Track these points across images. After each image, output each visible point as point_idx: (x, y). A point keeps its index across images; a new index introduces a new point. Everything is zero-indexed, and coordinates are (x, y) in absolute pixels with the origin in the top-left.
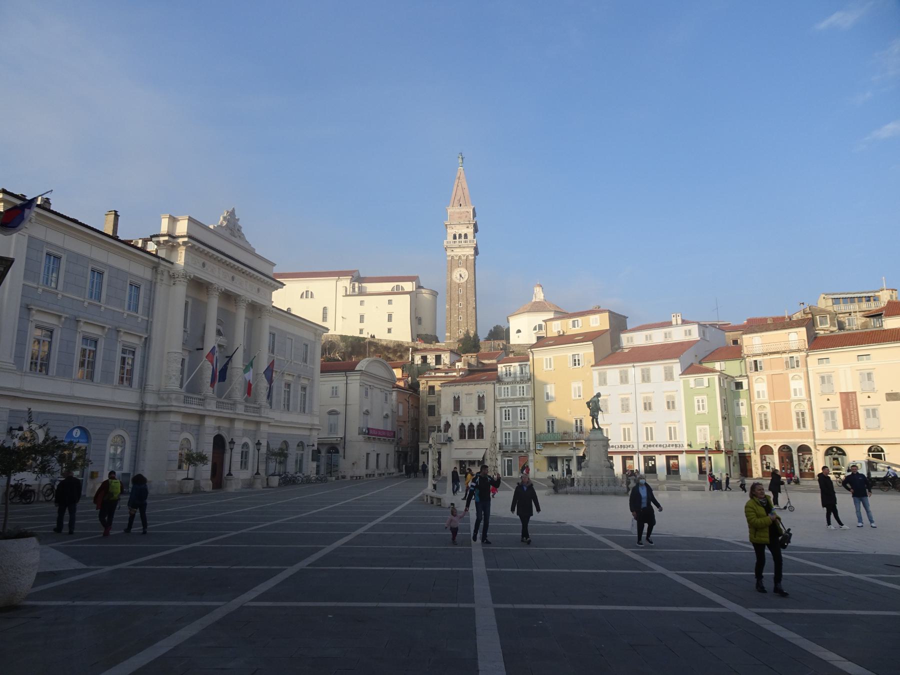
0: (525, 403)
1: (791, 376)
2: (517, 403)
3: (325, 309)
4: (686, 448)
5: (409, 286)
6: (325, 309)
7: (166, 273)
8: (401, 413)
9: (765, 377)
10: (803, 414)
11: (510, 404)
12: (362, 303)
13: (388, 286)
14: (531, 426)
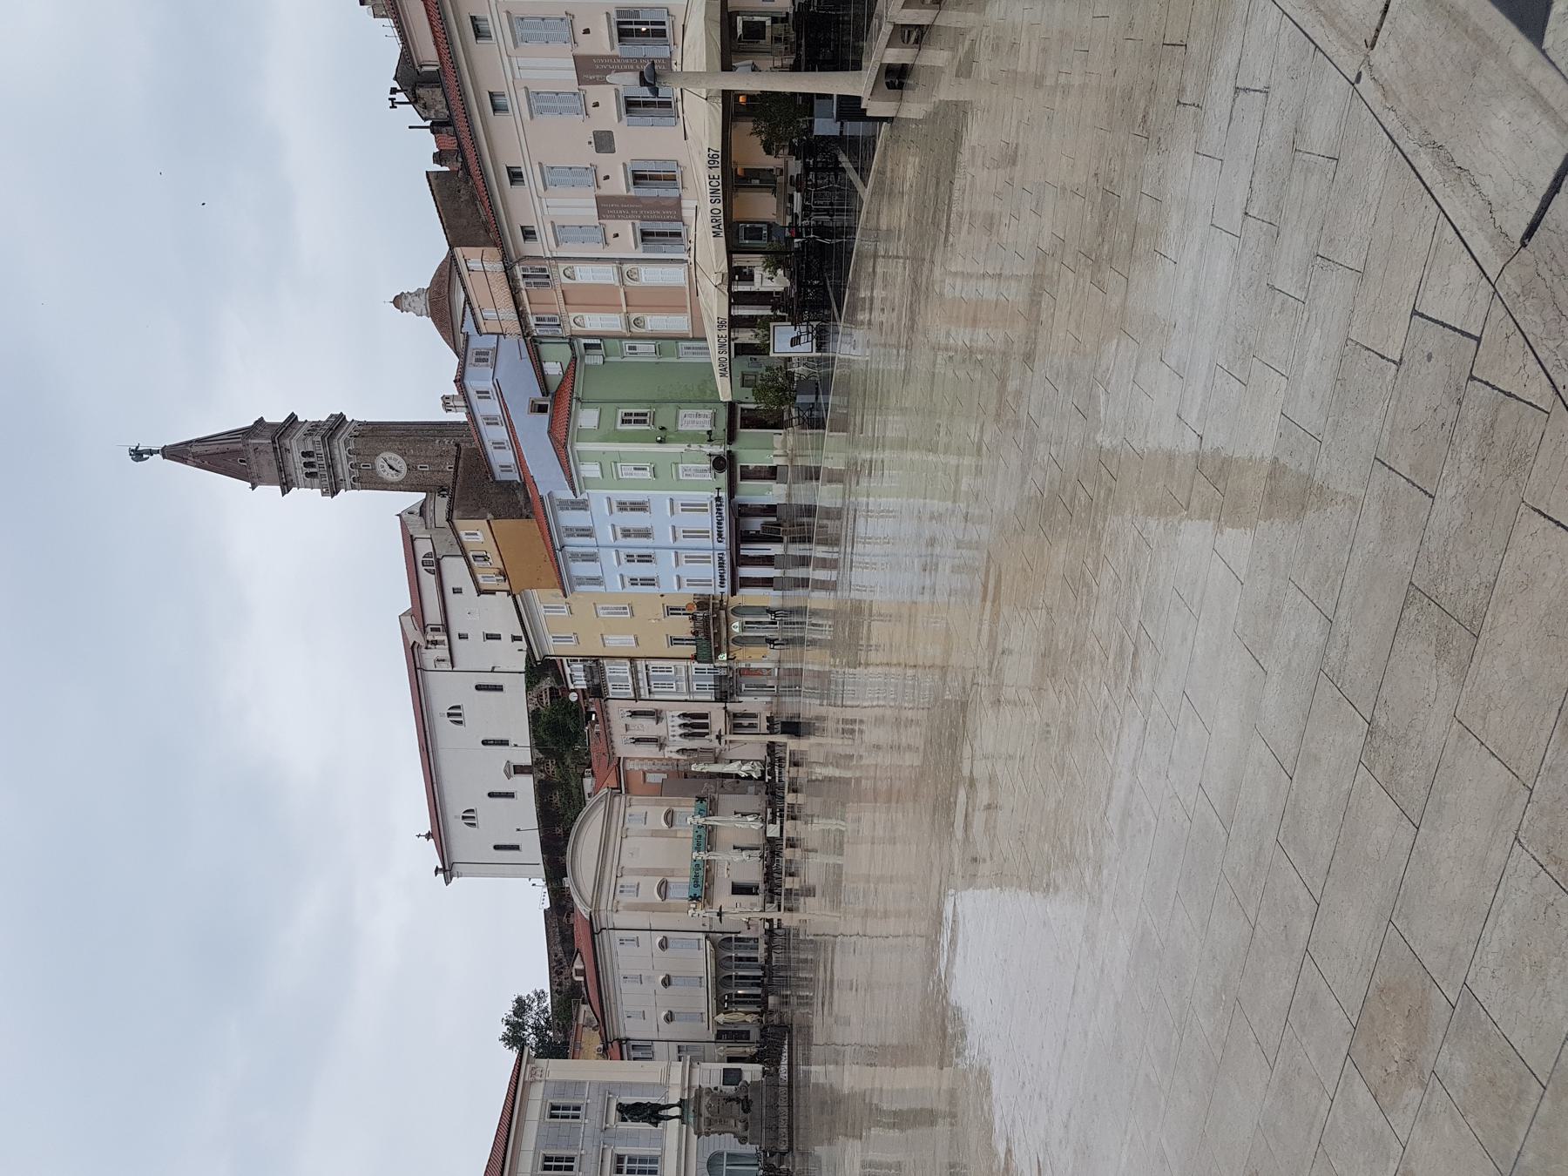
3: (478, 688)
4: (723, 494)
5: (423, 547)
6: (478, 688)
9: (572, 315)
11: (643, 684)
12: (462, 637)
13: (428, 581)
14: (684, 663)
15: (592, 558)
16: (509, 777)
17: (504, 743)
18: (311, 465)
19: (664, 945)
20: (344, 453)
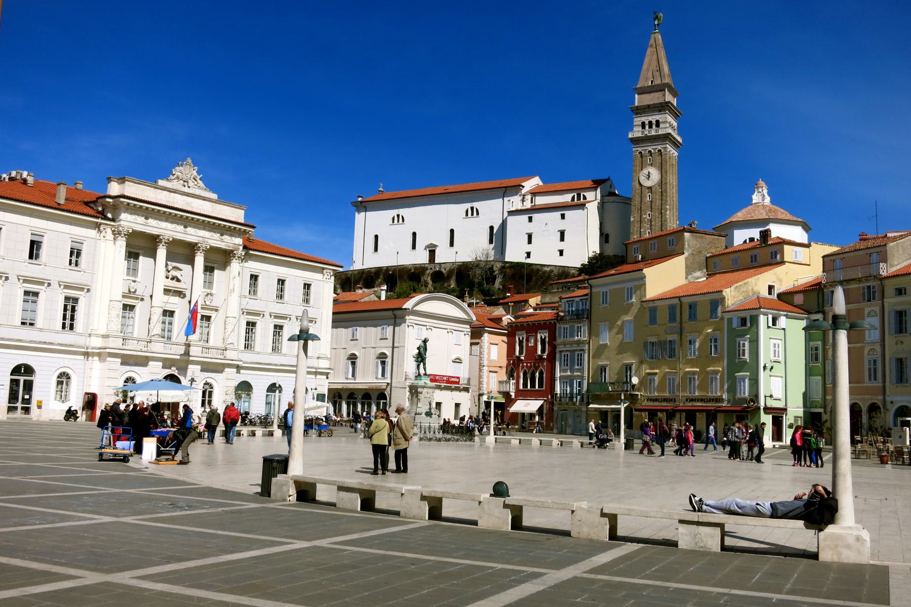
1: (867, 310)
2: (575, 347)
7: (109, 231)
10: (875, 361)
12: (530, 219)
13: (567, 198)
14: (586, 375)
15: (672, 318)
16: (427, 247)
17: (452, 244)
18: (651, 127)
19: (382, 357)
20: (659, 147)
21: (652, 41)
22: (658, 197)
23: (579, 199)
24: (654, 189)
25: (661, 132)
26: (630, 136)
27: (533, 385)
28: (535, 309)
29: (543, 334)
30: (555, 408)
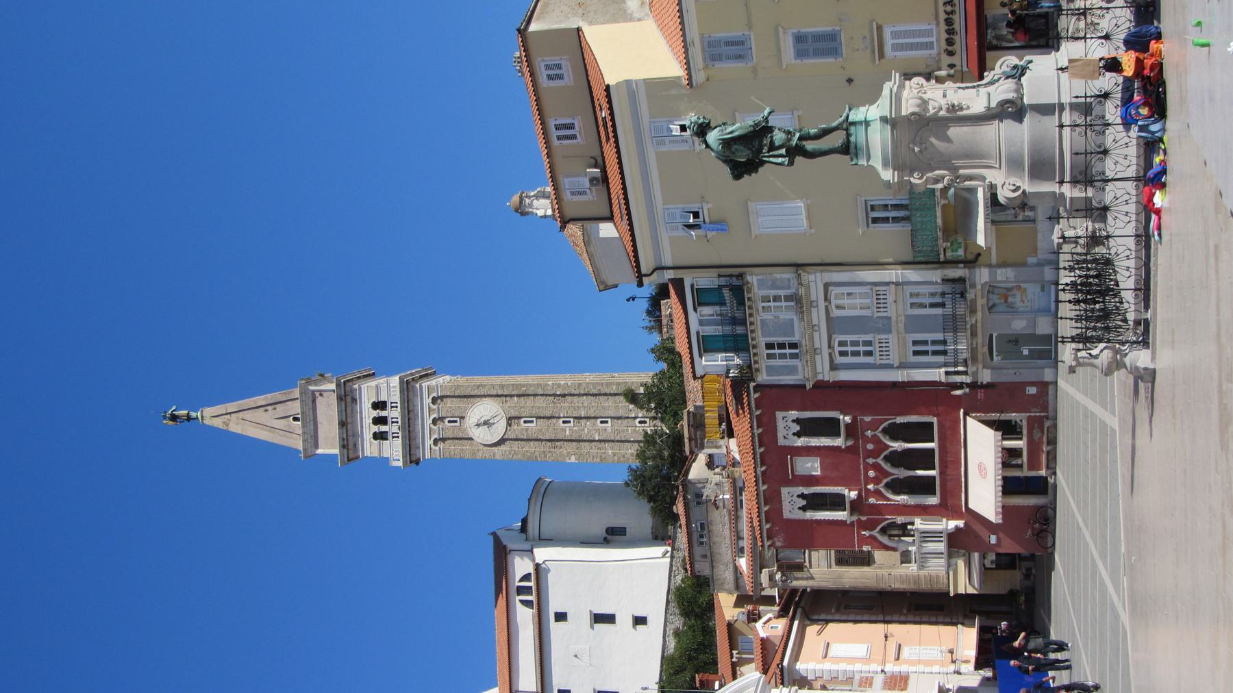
0: (817, 293)
8: (860, 650)
13: (525, 617)
20: (427, 401)
21: (218, 423)
22: (529, 402)
23: (527, 590)
24: (513, 413)
25: (396, 397)
26: (400, 464)
27: (925, 459)
28: (741, 550)
29: (786, 423)
30: (986, 377)
